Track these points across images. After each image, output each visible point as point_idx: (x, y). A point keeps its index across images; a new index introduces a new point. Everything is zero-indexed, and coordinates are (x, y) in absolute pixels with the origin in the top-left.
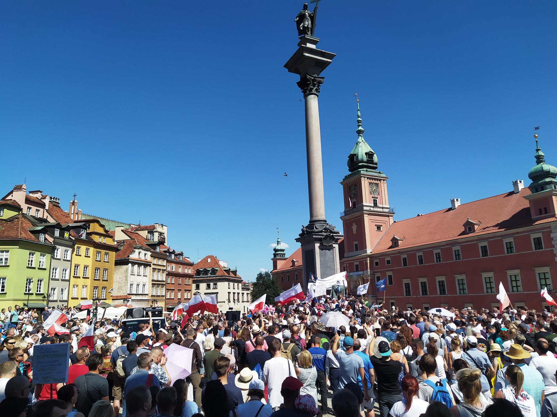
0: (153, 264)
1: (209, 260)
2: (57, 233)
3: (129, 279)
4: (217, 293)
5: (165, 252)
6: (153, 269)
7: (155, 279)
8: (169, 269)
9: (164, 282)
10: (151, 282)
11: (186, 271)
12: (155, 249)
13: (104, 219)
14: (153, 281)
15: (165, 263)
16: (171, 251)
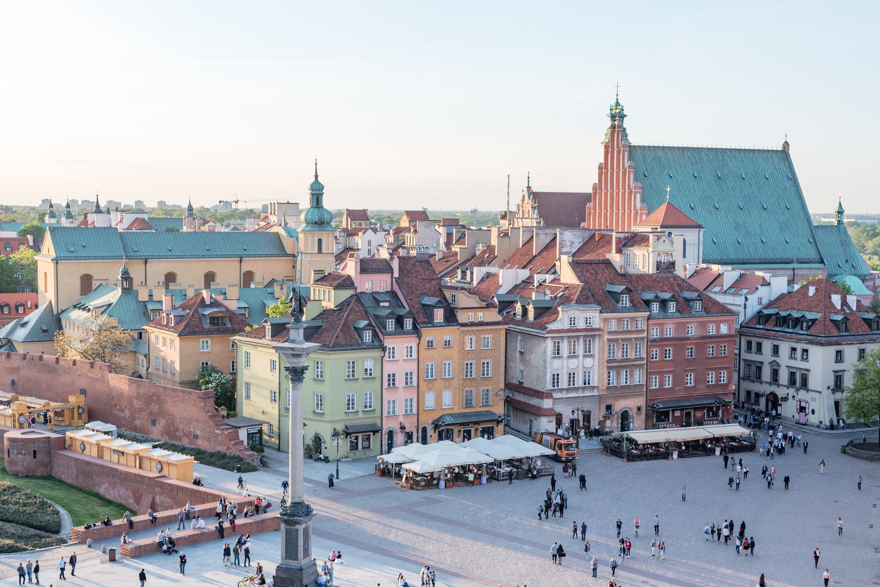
0: (610, 333)
1: (812, 291)
2: (391, 324)
3: (548, 365)
4: (808, 370)
5: (648, 303)
6: (609, 340)
7: (619, 355)
8: (655, 333)
9: (642, 359)
10: (605, 364)
11: (712, 330)
12: (618, 302)
13: (688, 149)
14: (608, 362)
15: (642, 325)
16: (666, 296)
